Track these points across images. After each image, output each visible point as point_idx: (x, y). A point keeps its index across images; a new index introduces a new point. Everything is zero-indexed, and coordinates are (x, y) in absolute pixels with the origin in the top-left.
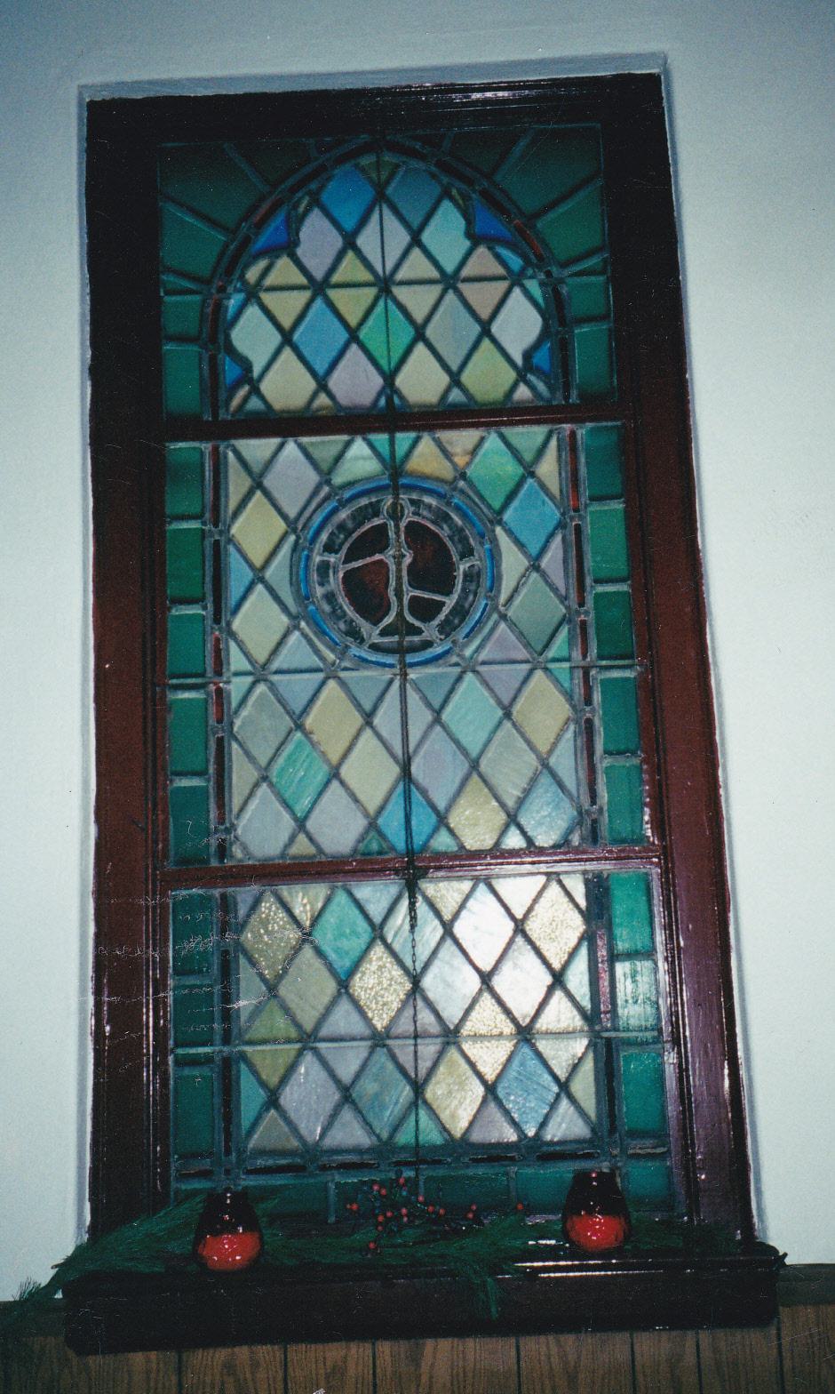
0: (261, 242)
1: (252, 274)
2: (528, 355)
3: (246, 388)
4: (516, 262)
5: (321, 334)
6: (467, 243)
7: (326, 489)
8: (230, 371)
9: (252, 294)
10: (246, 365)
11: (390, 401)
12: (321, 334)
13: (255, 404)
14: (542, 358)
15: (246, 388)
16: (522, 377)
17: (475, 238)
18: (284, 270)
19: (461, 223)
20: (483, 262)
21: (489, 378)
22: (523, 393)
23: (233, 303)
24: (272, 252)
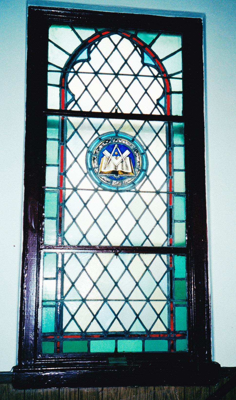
0: (80, 58)
1: (76, 67)
2: (158, 100)
3: (74, 102)
4: (156, 72)
5: (96, 88)
6: (142, 65)
7: (96, 135)
8: (69, 97)
9: (76, 73)
10: (73, 95)
11: (116, 110)
12: (96, 88)
13: (76, 109)
14: (162, 102)
15: (74, 102)
16: (156, 107)
17: (144, 65)
18: (86, 67)
19: (140, 59)
20: (146, 71)
21: (147, 108)
22: (156, 113)
23: (71, 75)
24: (83, 61)
